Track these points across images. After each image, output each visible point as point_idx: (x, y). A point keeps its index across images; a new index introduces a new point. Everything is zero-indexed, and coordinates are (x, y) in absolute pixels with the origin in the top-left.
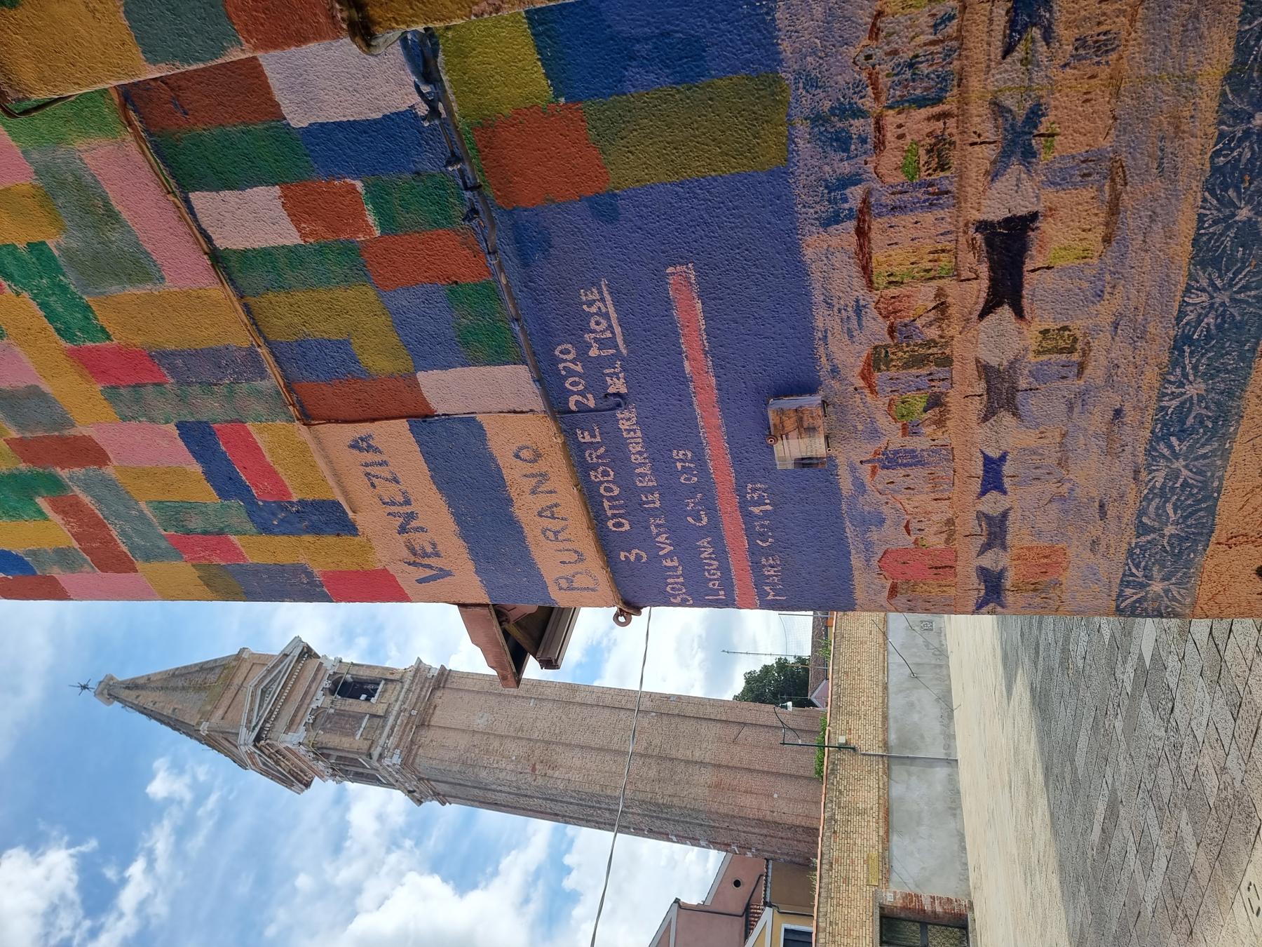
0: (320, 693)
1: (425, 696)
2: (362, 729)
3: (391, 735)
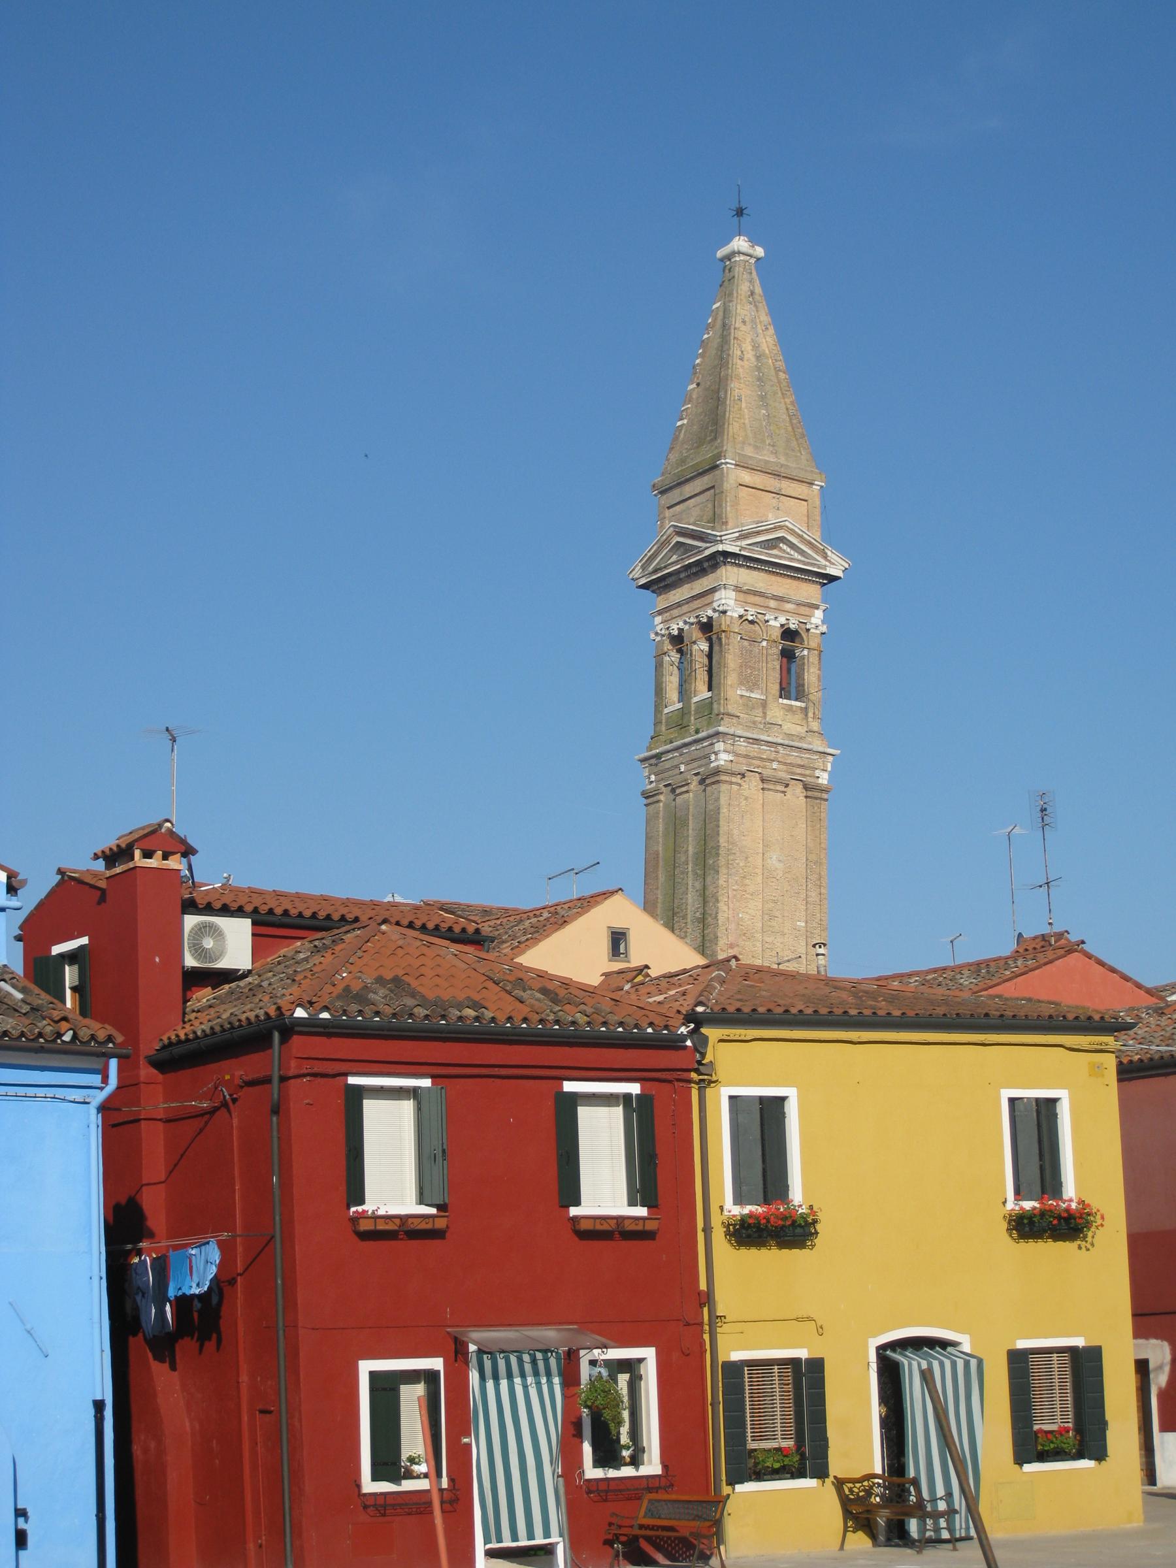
0: (782, 620)
3: (749, 743)
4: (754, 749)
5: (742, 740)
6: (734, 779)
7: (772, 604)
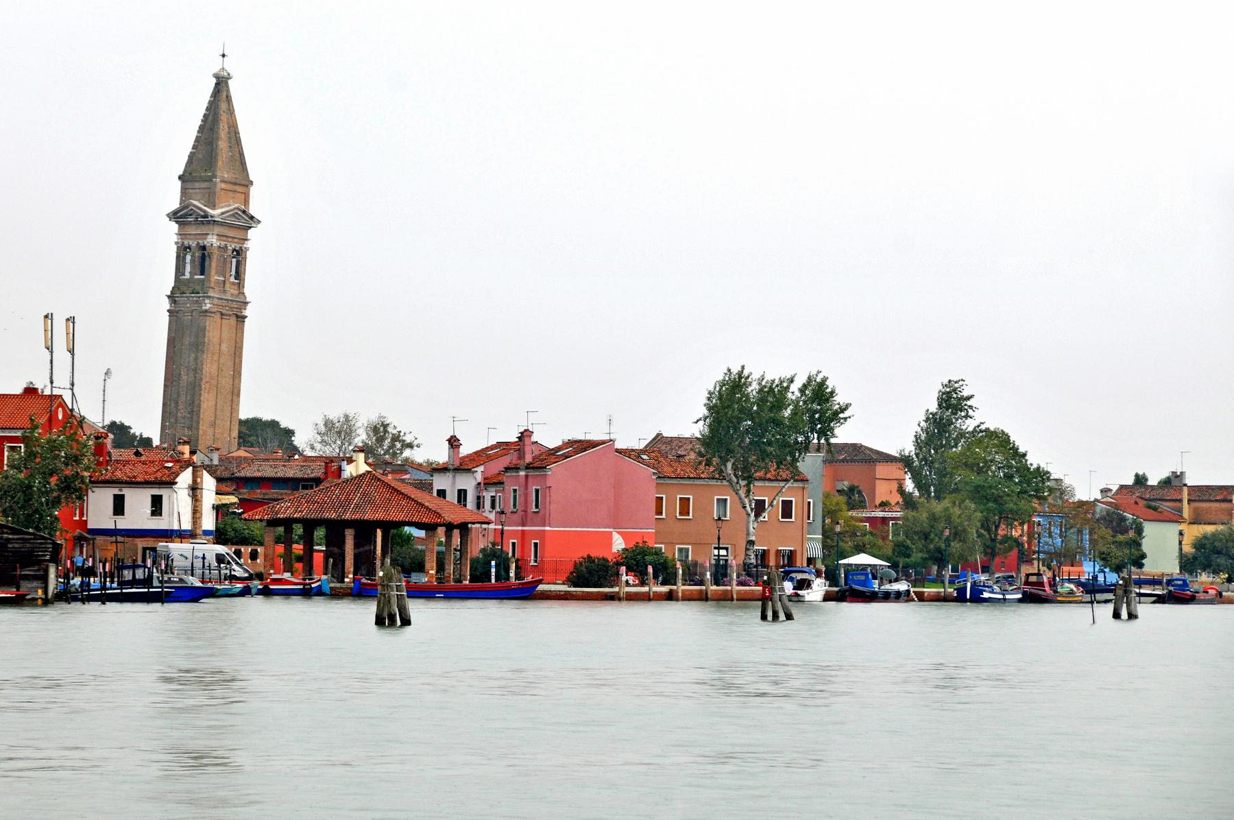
7: (230, 240)
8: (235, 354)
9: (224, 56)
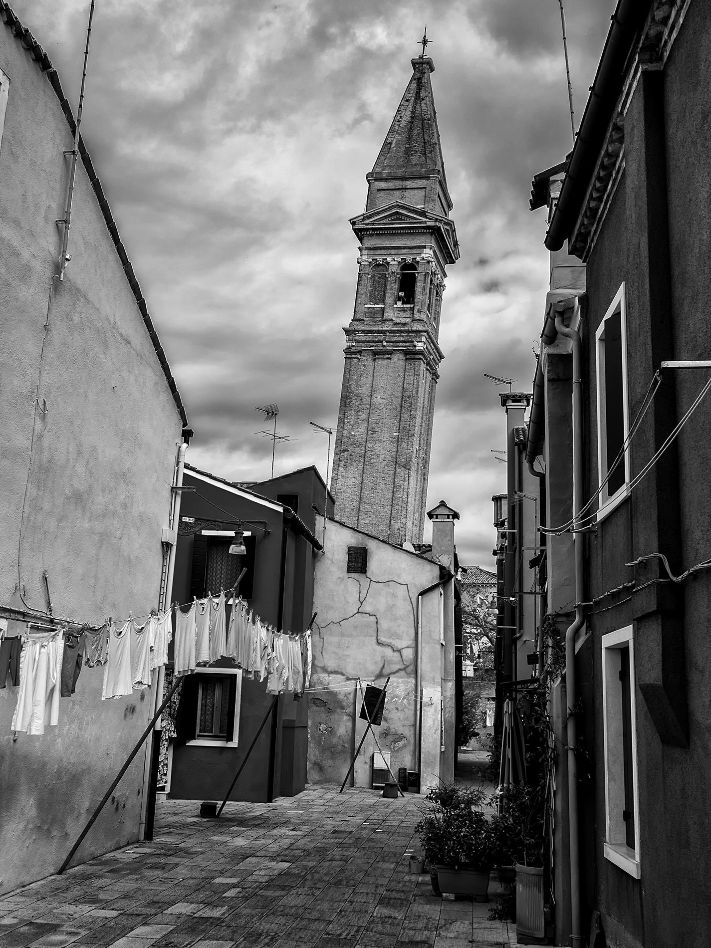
1: (398, 346)
2: (373, 306)
4: (369, 337)
5: (360, 333)
6: (354, 356)
7: (393, 252)
8: (401, 406)
9: (425, 42)
